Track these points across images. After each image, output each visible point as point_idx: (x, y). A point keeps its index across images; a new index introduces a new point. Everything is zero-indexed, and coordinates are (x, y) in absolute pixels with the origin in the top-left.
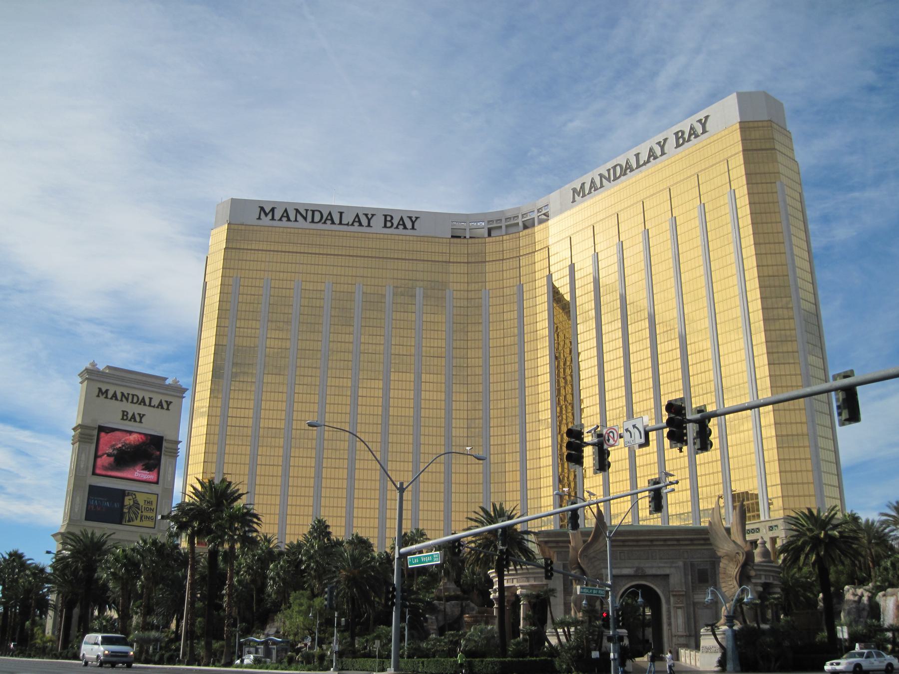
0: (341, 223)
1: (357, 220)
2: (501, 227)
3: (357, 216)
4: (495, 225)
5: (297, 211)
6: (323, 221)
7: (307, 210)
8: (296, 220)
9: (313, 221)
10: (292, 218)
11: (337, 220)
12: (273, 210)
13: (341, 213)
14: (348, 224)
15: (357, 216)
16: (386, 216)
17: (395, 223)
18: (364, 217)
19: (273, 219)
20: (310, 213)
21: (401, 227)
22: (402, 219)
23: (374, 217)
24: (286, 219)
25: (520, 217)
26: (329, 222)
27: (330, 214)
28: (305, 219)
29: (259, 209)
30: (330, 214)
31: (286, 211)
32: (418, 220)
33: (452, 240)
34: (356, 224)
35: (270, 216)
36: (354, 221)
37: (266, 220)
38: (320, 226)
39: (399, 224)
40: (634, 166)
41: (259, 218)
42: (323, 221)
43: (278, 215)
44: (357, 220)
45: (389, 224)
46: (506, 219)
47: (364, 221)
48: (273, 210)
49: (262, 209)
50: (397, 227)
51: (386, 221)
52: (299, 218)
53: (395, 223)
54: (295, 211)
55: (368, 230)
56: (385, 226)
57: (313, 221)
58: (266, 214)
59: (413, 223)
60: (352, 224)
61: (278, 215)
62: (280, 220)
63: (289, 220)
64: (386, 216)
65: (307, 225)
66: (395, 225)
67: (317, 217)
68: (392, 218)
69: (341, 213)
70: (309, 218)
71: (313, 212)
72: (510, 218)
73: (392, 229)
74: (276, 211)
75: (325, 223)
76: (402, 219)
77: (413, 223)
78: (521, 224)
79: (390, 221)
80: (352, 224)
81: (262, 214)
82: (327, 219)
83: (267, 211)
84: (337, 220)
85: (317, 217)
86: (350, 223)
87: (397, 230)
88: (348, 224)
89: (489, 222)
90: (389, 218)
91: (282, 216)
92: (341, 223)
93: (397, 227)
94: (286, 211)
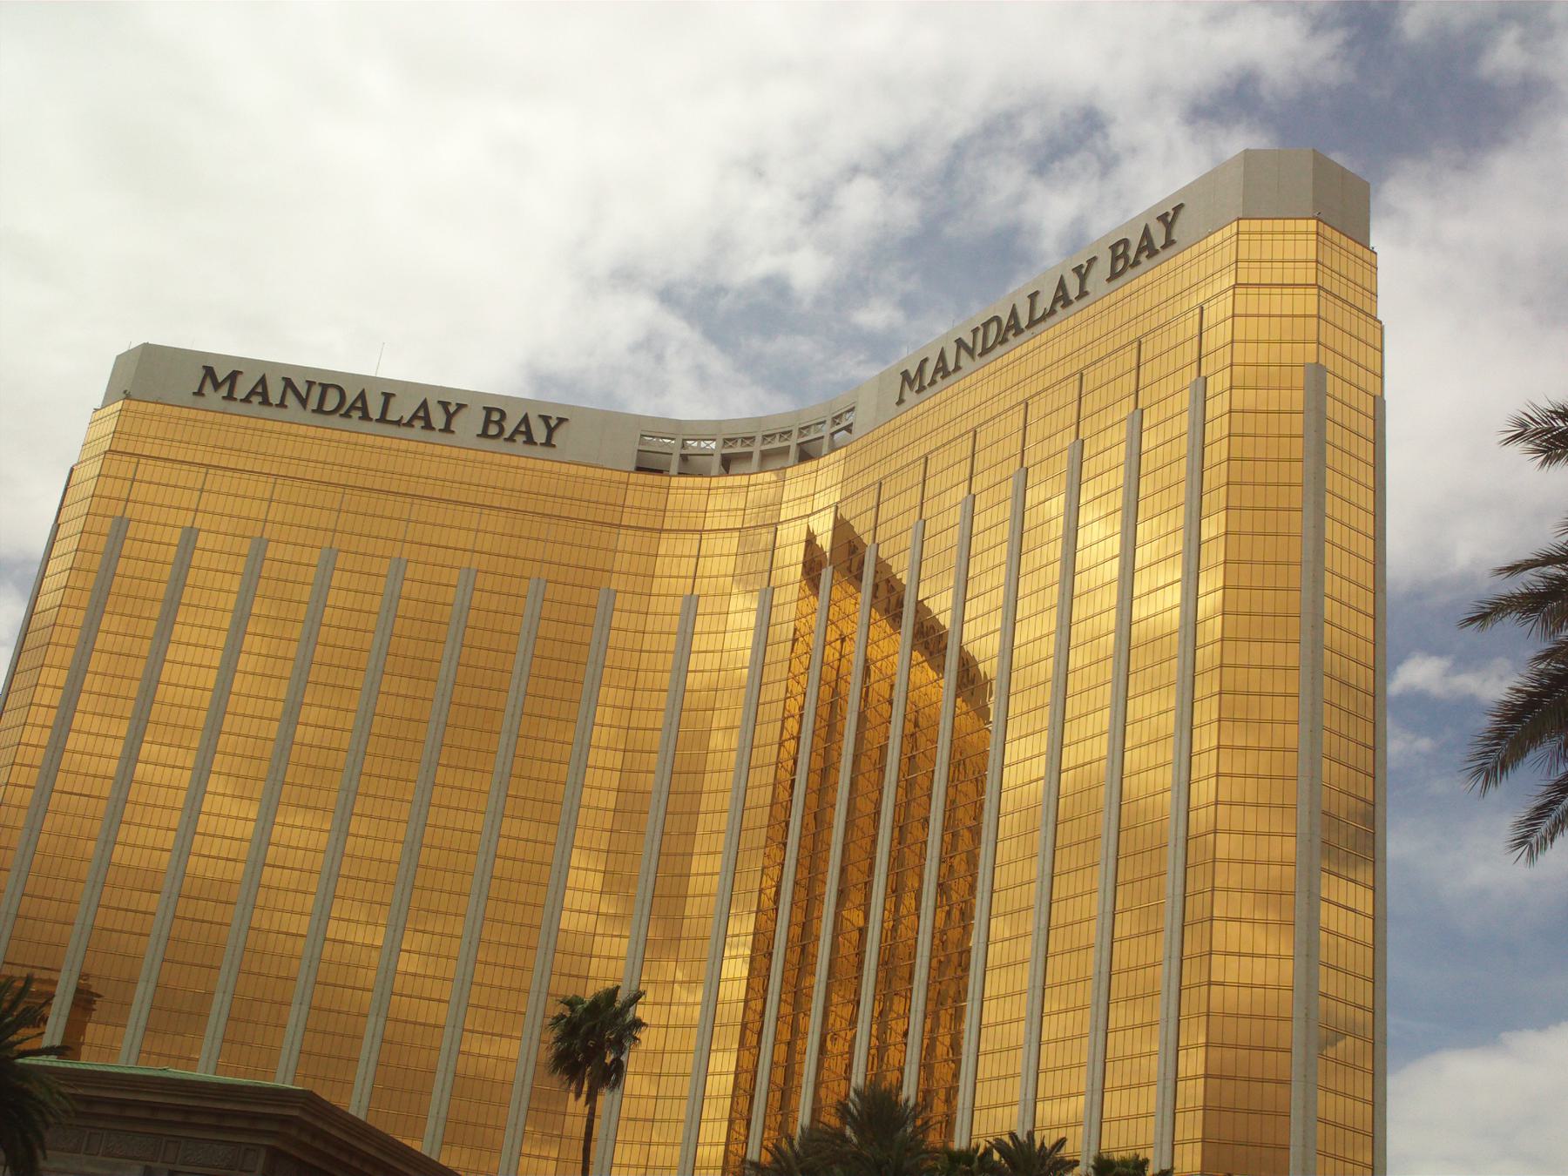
0: (383, 419)
1: (422, 415)
2: (749, 456)
3: (424, 405)
4: (738, 449)
5: (288, 383)
6: (342, 412)
7: (310, 384)
8: (282, 405)
9: (319, 410)
10: (275, 397)
11: (375, 412)
12: (234, 376)
13: (388, 397)
14: (398, 423)
15: (424, 405)
16: (489, 411)
17: (509, 427)
18: (440, 408)
19: (230, 397)
20: (316, 392)
21: (520, 438)
22: (525, 420)
23: (463, 413)
25: (795, 433)
26: (356, 414)
27: (362, 396)
28: (303, 402)
29: (202, 373)
30: (362, 396)
31: (263, 381)
32: (564, 426)
33: (634, 477)
34: (418, 424)
35: (224, 391)
36: (415, 416)
37: (214, 397)
38: (336, 420)
39: (516, 431)
40: (1024, 322)
41: (199, 393)
42: (342, 412)
43: (242, 390)
44: (421, 414)
45: (493, 430)
46: (765, 437)
47: (438, 419)
48: (234, 376)
49: (209, 372)
50: (511, 439)
51: (488, 422)
52: (291, 399)
53: (509, 427)
54: (283, 384)
55: (446, 438)
56: (484, 434)
57: (319, 410)
58: (217, 386)
60: (409, 424)
61: (242, 390)
62: (247, 400)
63: (266, 402)
64: (489, 411)
65: (306, 416)
66: (507, 434)
67: (332, 401)
68: (503, 414)
69: (388, 397)
70: (313, 402)
71: (325, 387)
72: (773, 435)
73: (500, 441)
74: (240, 379)
75: (347, 415)
76: (525, 420)
78: (793, 451)
79: (499, 423)
81: (208, 383)
82: (353, 407)
83: (220, 379)
84: (375, 412)
85: (332, 401)
86: (405, 421)
87: (509, 444)
88: (398, 423)
89: (726, 441)
90: (495, 417)
91: (253, 392)
92: (383, 419)
93: (511, 439)
94: (263, 381)
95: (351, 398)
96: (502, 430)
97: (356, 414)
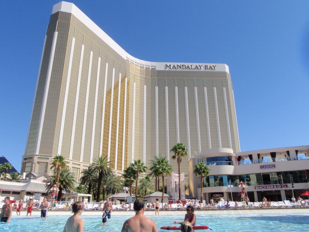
5: (178, 65)
8: (178, 68)
10: (176, 68)
13: (192, 65)
14: (194, 69)
18: (199, 66)
19: (170, 68)
24: (175, 68)
26: (188, 68)
28: (181, 68)
34: (197, 68)
39: (210, 68)
43: (172, 67)
48: (170, 65)
49: (167, 65)
51: (206, 67)
52: (179, 67)
57: (183, 68)
58: (168, 67)
59: (214, 67)
60: (195, 69)
61: (172, 67)
62: (173, 68)
64: (206, 66)
71: (183, 65)
75: (187, 69)
77: (214, 67)
79: (207, 67)
80: (195, 69)
81: (167, 67)
84: (190, 68)
90: (207, 66)
95: (186, 66)
96: (208, 68)
97: (188, 68)
